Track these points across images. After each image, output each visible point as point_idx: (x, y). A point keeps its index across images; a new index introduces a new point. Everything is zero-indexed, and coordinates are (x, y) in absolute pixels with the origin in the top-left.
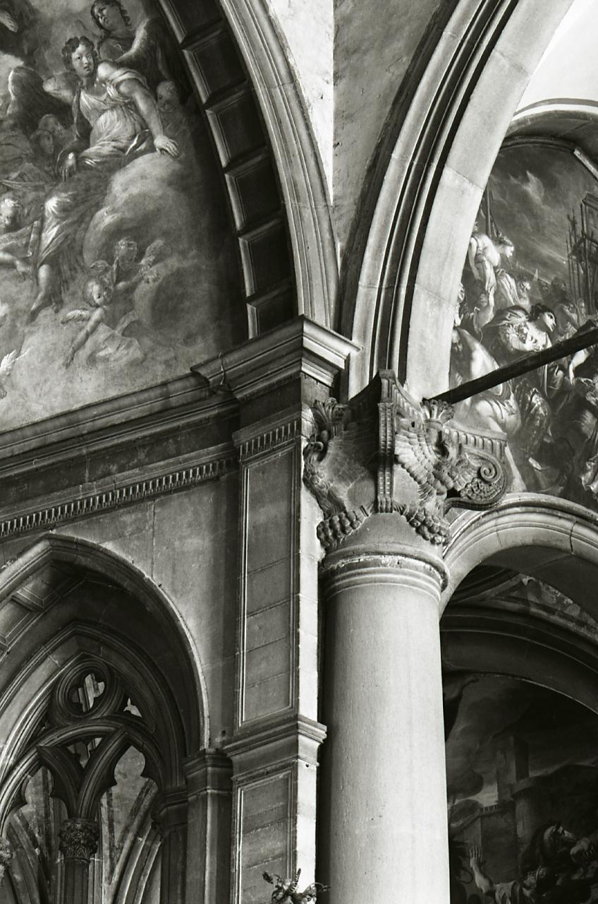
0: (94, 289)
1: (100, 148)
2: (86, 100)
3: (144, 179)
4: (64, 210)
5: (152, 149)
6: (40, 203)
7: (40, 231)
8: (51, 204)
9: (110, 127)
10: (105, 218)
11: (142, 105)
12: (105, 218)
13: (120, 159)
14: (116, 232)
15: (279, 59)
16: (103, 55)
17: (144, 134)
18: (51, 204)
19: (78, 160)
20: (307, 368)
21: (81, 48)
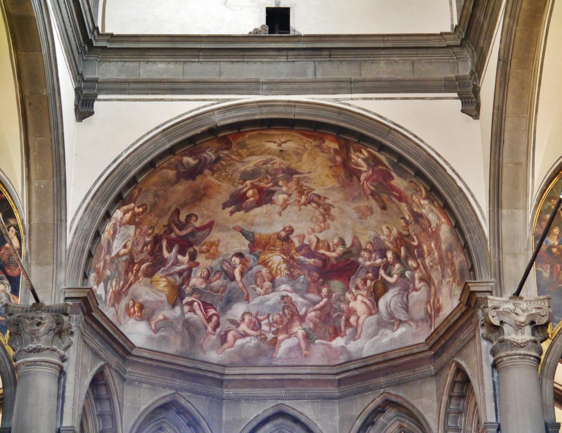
0: (449, 270)
1: (433, 225)
2: (424, 211)
3: (445, 231)
4: (436, 246)
5: (442, 223)
6: (430, 245)
7: (434, 254)
8: (433, 245)
9: (432, 217)
10: (444, 247)
11: (434, 210)
12: (444, 247)
13: (438, 227)
14: (447, 251)
15: (455, 185)
16: (419, 197)
17: (439, 219)
18: (433, 245)
19: (431, 229)
20: (479, 295)
21: (414, 197)
